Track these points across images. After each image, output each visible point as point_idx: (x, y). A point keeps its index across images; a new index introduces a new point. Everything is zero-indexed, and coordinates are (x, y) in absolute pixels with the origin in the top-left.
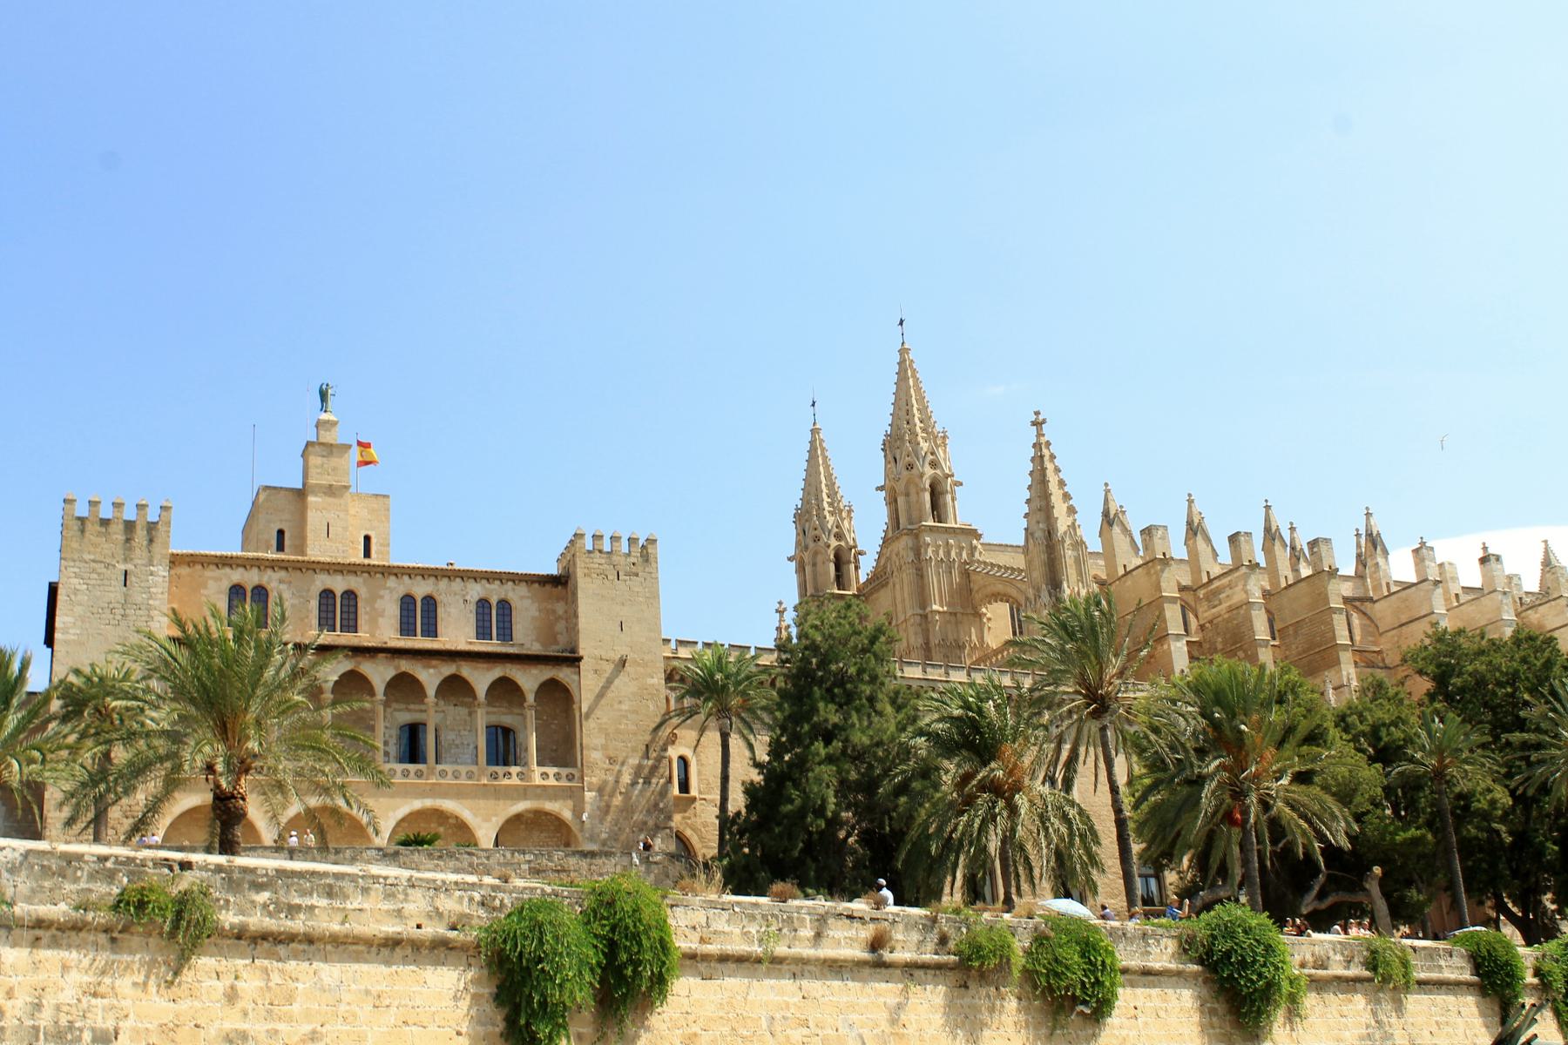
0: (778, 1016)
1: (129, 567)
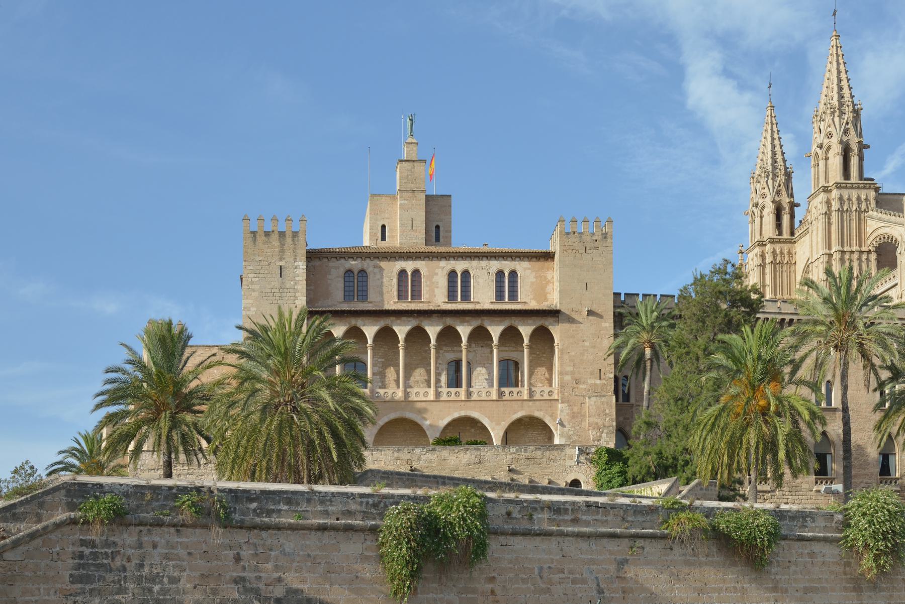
0: (546, 566)
1: (282, 263)
